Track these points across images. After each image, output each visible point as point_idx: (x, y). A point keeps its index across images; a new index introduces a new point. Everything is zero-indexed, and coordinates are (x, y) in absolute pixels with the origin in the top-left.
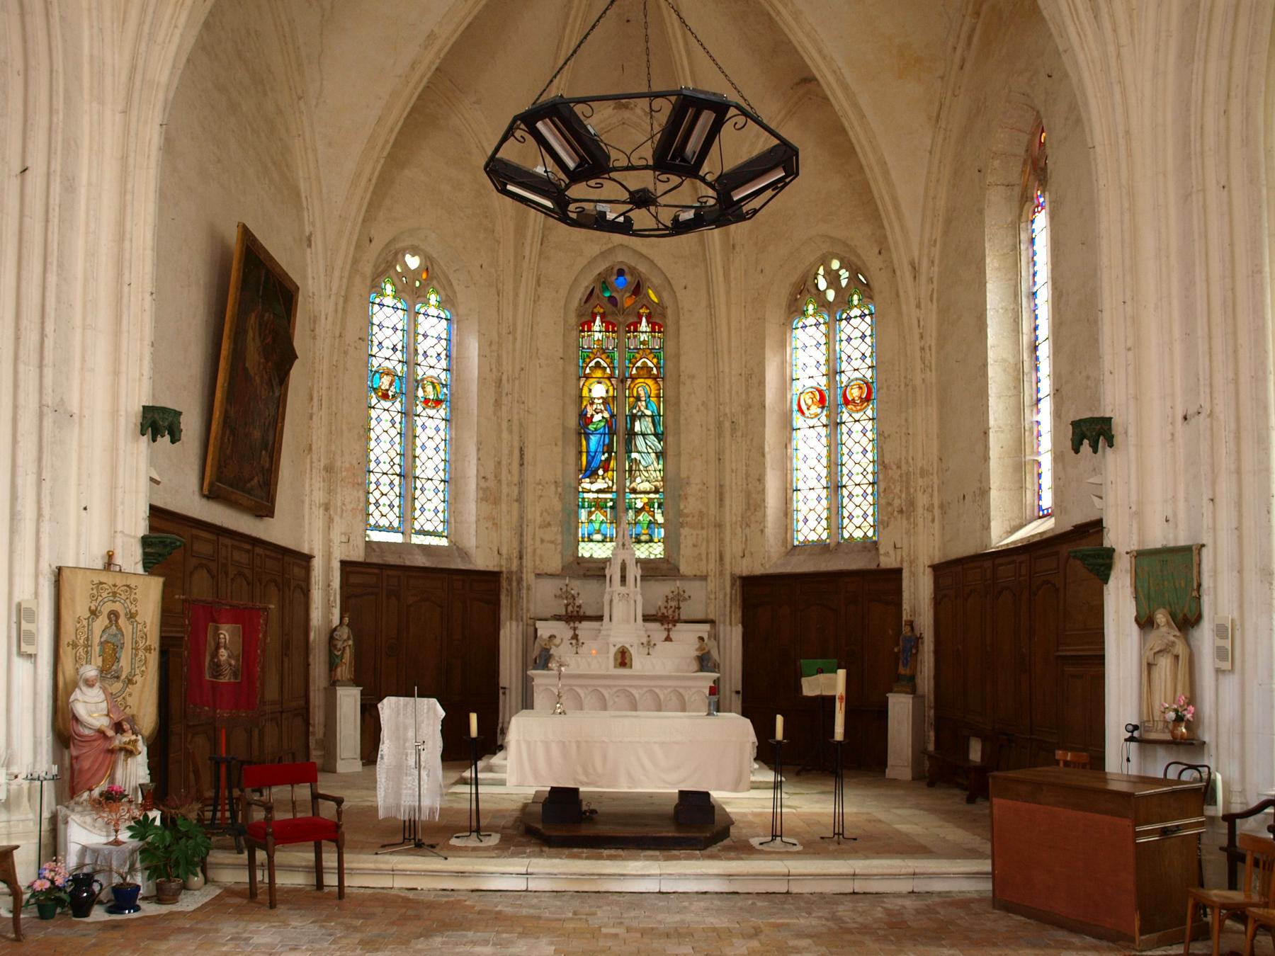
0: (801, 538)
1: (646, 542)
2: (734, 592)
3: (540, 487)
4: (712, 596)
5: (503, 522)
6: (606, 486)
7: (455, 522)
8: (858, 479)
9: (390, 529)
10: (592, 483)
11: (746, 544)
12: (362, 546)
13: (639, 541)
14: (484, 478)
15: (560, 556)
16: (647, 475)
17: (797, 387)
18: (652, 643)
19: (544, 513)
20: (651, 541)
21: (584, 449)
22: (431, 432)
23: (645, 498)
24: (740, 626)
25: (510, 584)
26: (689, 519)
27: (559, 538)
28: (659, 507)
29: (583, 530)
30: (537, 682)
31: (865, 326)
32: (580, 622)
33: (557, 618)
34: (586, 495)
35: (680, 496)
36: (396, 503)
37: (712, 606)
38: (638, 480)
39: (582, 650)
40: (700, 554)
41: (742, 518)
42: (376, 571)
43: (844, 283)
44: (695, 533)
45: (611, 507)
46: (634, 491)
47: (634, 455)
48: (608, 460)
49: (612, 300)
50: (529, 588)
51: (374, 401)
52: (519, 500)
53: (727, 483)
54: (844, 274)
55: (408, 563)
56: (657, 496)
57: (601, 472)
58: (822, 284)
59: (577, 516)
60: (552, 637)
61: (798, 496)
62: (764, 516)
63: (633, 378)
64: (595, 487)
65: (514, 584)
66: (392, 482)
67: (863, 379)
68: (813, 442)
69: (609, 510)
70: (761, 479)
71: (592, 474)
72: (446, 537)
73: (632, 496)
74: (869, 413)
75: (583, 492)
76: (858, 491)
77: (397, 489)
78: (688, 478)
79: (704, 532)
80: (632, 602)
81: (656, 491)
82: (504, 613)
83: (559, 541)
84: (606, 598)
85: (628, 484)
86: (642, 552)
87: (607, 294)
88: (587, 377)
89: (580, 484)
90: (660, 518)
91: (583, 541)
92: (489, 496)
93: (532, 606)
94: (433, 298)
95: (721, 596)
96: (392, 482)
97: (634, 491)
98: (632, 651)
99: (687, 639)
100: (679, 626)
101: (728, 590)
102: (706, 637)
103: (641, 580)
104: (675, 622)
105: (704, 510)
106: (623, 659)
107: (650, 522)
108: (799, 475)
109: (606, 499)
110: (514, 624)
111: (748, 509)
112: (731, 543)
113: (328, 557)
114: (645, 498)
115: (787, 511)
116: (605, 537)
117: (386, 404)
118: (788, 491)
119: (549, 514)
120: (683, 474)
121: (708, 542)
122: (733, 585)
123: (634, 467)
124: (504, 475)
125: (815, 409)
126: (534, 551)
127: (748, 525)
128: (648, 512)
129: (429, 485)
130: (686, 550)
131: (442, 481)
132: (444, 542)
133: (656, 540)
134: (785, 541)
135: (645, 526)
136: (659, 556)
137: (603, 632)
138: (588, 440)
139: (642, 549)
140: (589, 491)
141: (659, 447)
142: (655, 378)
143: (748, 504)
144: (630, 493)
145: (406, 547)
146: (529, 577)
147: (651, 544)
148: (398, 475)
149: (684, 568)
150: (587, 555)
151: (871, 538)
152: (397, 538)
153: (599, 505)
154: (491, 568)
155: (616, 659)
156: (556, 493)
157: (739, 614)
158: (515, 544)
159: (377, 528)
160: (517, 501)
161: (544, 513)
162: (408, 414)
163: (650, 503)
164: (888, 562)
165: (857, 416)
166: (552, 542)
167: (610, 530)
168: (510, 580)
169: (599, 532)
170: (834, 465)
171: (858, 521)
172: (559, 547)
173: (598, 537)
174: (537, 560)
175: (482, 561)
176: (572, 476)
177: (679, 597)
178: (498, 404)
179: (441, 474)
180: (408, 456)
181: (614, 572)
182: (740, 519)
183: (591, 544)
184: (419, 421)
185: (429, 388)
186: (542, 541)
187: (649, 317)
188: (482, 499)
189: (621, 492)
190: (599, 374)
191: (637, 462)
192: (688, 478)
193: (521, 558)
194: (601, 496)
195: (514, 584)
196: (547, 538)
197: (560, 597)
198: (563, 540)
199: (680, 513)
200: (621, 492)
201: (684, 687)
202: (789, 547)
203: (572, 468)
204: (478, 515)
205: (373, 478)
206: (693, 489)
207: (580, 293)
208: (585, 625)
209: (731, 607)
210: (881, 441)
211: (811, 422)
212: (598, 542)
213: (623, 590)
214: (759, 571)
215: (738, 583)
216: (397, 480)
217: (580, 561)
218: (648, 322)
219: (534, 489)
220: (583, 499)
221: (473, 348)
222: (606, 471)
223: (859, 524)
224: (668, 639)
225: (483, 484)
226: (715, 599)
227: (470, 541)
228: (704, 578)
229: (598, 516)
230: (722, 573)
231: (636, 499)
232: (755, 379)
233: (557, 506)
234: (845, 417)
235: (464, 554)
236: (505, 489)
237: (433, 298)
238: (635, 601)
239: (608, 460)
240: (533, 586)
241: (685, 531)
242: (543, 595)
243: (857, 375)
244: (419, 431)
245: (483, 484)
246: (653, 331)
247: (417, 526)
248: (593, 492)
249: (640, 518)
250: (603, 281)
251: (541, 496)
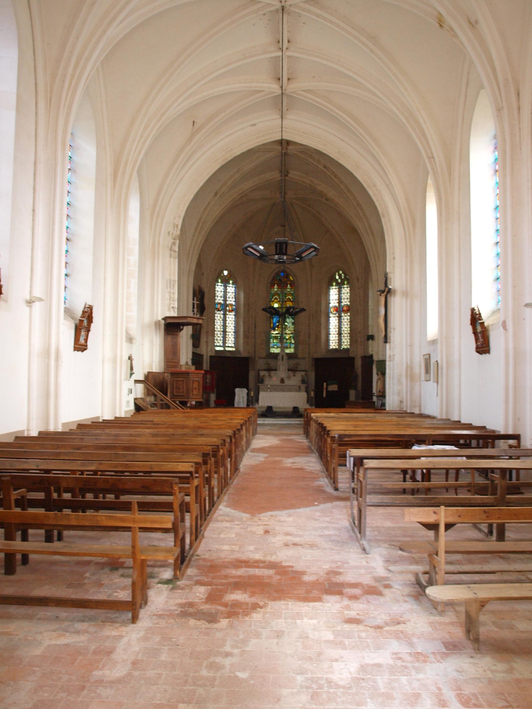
8: (346, 332)
9: (220, 346)
12: (214, 351)
13: (287, 348)
17: (331, 305)
20: (290, 348)
21: (272, 322)
22: (231, 319)
29: (271, 345)
30: (260, 387)
31: (348, 290)
33: (265, 370)
38: (287, 331)
43: (343, 277)
46: (286, 334)
47: (286, 324)
49: (280, 280)
51: (216, 312)
52: (255, 337)
54: (343, 275)
57: (276, 328)
58: (337, 277)
59: (270, 341)
60: (264, 375)
61: (331, 336)
63: (286, 302)
67: (347, 305)
68: (335, 321)
69: (279, 339)
70: (320, 332)
71: (274, 330)
74: (349, 314)
76: (346, 335)
81: (292, 334)
82: (250, 369)
86: (287, 351)
87: (278, 278)
88: (273, 301)
90: (293, 342)
92: (246, 336)
94: (231, 282)
97: (286, 334)
99: (299, 376)
102: (304, 375)
106: (282, 381)
108: (331, 330)
113: (207, 355)
115: (328, 340)
117: (219, 312)
118: (328, 334)
125: (335, 312)
129: (230, 334)
132: (234, 349)
138: (273, 319)
141: (293, 321)
142: (291, 301)
145: (225, 351)
146: (257, 358)
149: (299, 356)
150: (272, 352)
152: (222, 349)
153: (276, 338)
159: (217, 346)
162: (225, 315)
163: (290, 337)
164: (352, 355)
165: (346, 315)
167: (279, 345)
169: (276, 345)
170: (340, 328)
171: (346, 343)
173: (276, 347)
175: (244, 355)
177: (298, 364)
178: (248, 311)
180: (225, 326)
181: (280, 357)
183: (274, 349)
184: (227, 316)
185: (230, 307)
187: (290, 284)
189: (282, 334)
190: (276, 301)
191: (286, 325)
193: (255, 353)
194: (277, 335)
200: (282, 334)
205: (216, 333)
207: (271, 278)
210: (351, 322)
211: (334, 315)
213: (282, 363)
216: (222, 333)
218: (290, 286)
221: (242, 295)
222: (278, 328)
223: (346, 344)
224: (294, 376)
227: (241, 349)
228: (304, 358)
232: (318, 303)
234: (343, 314)
237: (231, 282)
239: (278, 325)
242: (261, 364)
243: (346, 303)
244: (227, 319)
246: (291, 288)
250: (278, 274)
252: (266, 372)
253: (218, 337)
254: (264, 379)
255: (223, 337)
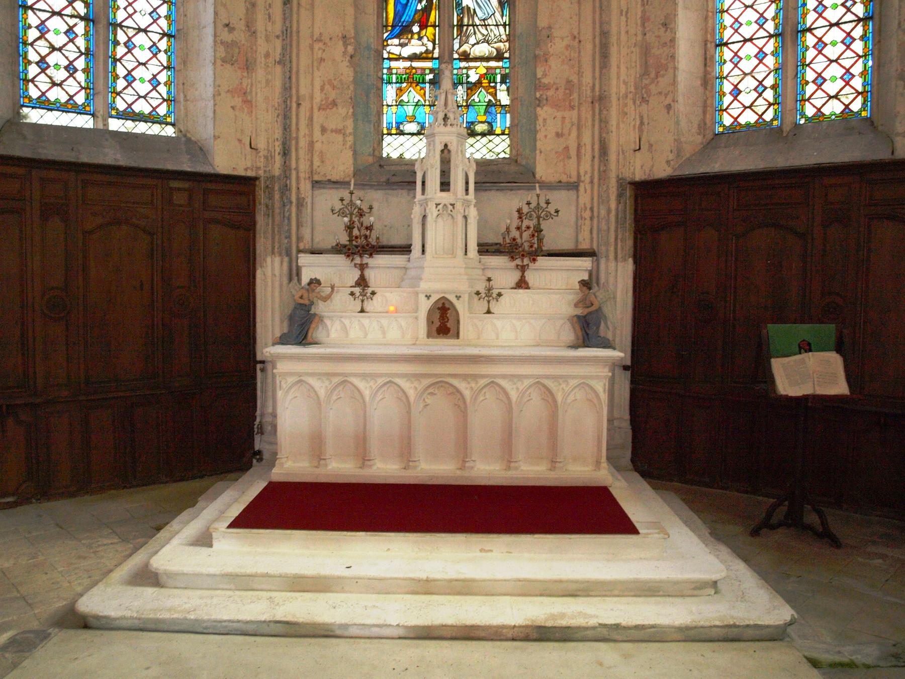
0: (727, 121)
1: (483, 135)
2: (621, 206)
3: (321, 45)
4: (587, 214)
5: (260, 98)
6: (423, 49)
7: (186, 100)
9: (69, 107)
10: (402, 45)
11: (641, 130)
14: (227, 25)
15: (349, 154)
16: (485, 32)
18: (495, 292)
19: (327, 87)
20: (491, 132)
23: (482, 67)
24: (631, 261)
25: (271, 197)
26: (550, 93)
27: (350, 123)
28: (503, 81)
29: (389, 116)
30: (282, 367)
32: (371, 255)
33: (338, 249)
34: (394, 64)
35: (536, 57)
36: (80, 64)
37: (586, 228)
38: (472, 40)
39: (372, 305)
40: (567, 148)
41: (636, 88)
42: (21, 171)
44: (559, 114)
45: (432, 82)
46: (465, 57)
48: (427, 10)
50: (300, 204)
53: (614, 30)
55: (84, 159)
56: (500, 64)
57: (416, 29)
62: (674, 83)
64: (406, 52)
65: (277, 196)
66: (70, 30)
69: (427, 85)
70: (668, 24)
71: (403, 31)
72: (173, 125)
73: (463, 64)
75: (390, 59)
77: (81, 42)
78: (550, 28)
79: (575, 113)
80: (460, 220)
81: (499, 57)
82: (262, 243)
83: (350, 130)
84: (417, 211)
85: (456, 46)
89: (384, 47)
90: (504, 98)
91: (390, 134)
93: (306, 232)
95: (603, 212)
96: (70, 30)
97: (465, 57)
98: (459, 305)
100: (542, 261)
101: (613, 205)
103: (476, 190)
104: (535, 254)
105: (574, 78)
107: (489, 104)
109: (423, 69)
110: (277, 260)
111: (645, 73)
112: (618, 127)
114: (482, 67)
116: (423, 128)
119: (334, 88)
120: (542, 22)
121: (579, 128)
122: (620, 196)
123: (465, 21)
124: (260, 24)
126: (311, 144)
127: (644, 100)
128: (485, 88)
130: (546, 142)
131: (164, 35)
132: (169, 131)
133: (498, 131)
134: (703, 127)
135: (482, 109)
136: (502, 155)
137: (412, 273)
139: (478, 146)
140: (399, 58)
143: (645, 66)
144: (460, 60)
147: (491, 137)
148: (82, 18)
149: (543, 171)
150: (395, 155)
151: (858, 113)
154: (241, 172)
155: (430, 322)
156: (345, 53)
157: (630, 243)
158: (278, 133)
159: (44, 103)
160: (279, 63)
161: (327, 87)
163: (490, 74)
166: (337, 131)
168: (269, 189)
169: (412, 119)
171: (831, 88)
172: (350, 140)
173: (412, 127)
174: (317, 162)
176: (373, 32)
179: (163, 23)
182: (632, 89)
183: (402, 138)
186: (324, 130)
188: (224, 61)
192: (550, 28)
193: (285, 153)
194: (416, 64)
195: (277, 196)
196: (331, 125)
197: (342, 213)
198: (355, 128)
199: (536, 85)
200: (446, 57)
201: (555, 378)
202: (709, 136)
203: (371, 20)
204: (217, 86)
206: (557, 46)
208: (381, 260)
209: (616, 231)
212: (412, 134)
213: (445, 198)
214: (662, 171)
215: (628, 193)
216: (80, 28)
217: (384, 163)
219: (312, 49)
220: (390, 69)
224: (522, 284)
225: (226, 36)
226: (592, 218)
227: (204, 130)
228: (574, 186)
229: (412, 95)
230: (603, 175)
231: (468, 68)
233: (347, 73)
235: (194, 148)
236: (262, 46)
238: (465, 217)
239: (427, 10)
240: (309, 200)
241: (543, 112)
245: (226, 36)
247: (121, 105)
248: (404, 59)
249: (475, 98)
251: (322, 60)
252: (340, 260)
253: (53, 49)
254: (320, 308)
255: (87, 53)
